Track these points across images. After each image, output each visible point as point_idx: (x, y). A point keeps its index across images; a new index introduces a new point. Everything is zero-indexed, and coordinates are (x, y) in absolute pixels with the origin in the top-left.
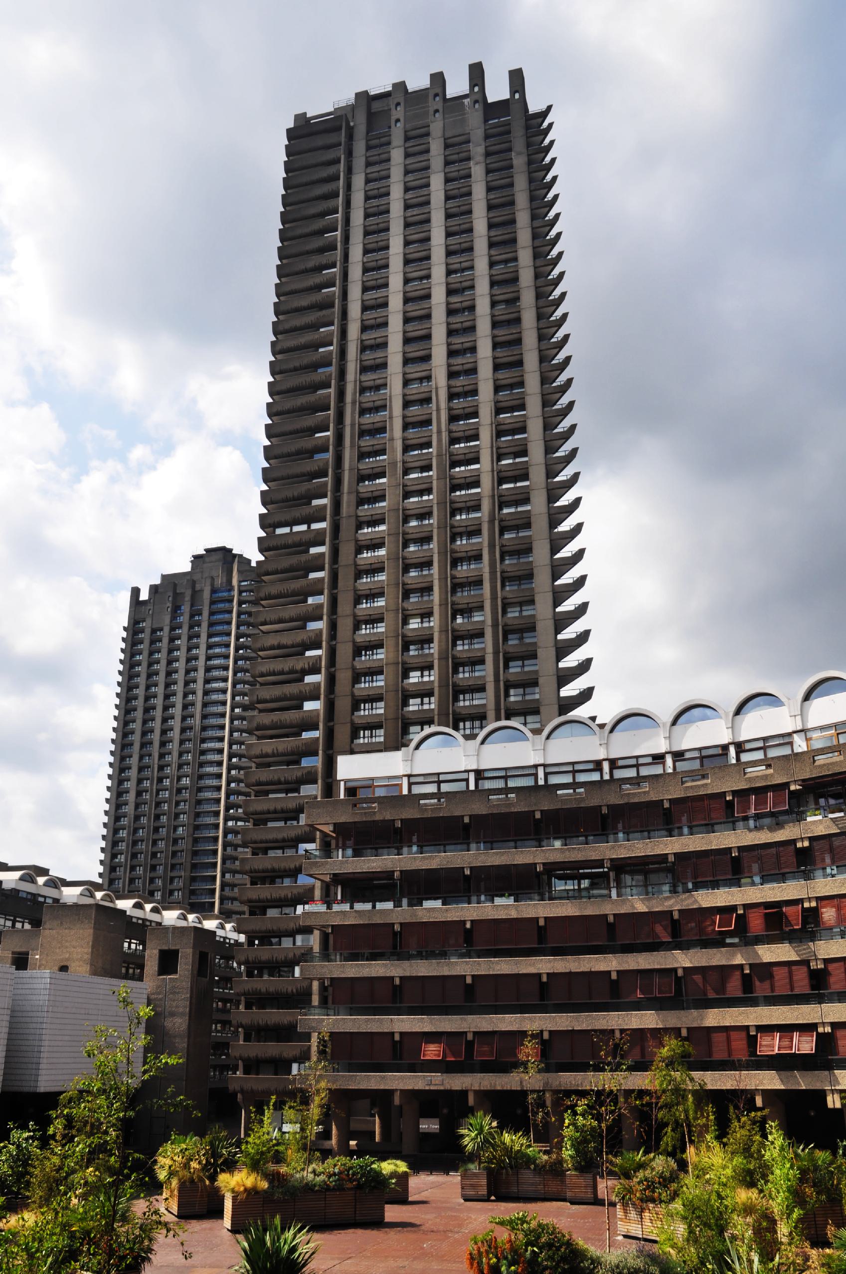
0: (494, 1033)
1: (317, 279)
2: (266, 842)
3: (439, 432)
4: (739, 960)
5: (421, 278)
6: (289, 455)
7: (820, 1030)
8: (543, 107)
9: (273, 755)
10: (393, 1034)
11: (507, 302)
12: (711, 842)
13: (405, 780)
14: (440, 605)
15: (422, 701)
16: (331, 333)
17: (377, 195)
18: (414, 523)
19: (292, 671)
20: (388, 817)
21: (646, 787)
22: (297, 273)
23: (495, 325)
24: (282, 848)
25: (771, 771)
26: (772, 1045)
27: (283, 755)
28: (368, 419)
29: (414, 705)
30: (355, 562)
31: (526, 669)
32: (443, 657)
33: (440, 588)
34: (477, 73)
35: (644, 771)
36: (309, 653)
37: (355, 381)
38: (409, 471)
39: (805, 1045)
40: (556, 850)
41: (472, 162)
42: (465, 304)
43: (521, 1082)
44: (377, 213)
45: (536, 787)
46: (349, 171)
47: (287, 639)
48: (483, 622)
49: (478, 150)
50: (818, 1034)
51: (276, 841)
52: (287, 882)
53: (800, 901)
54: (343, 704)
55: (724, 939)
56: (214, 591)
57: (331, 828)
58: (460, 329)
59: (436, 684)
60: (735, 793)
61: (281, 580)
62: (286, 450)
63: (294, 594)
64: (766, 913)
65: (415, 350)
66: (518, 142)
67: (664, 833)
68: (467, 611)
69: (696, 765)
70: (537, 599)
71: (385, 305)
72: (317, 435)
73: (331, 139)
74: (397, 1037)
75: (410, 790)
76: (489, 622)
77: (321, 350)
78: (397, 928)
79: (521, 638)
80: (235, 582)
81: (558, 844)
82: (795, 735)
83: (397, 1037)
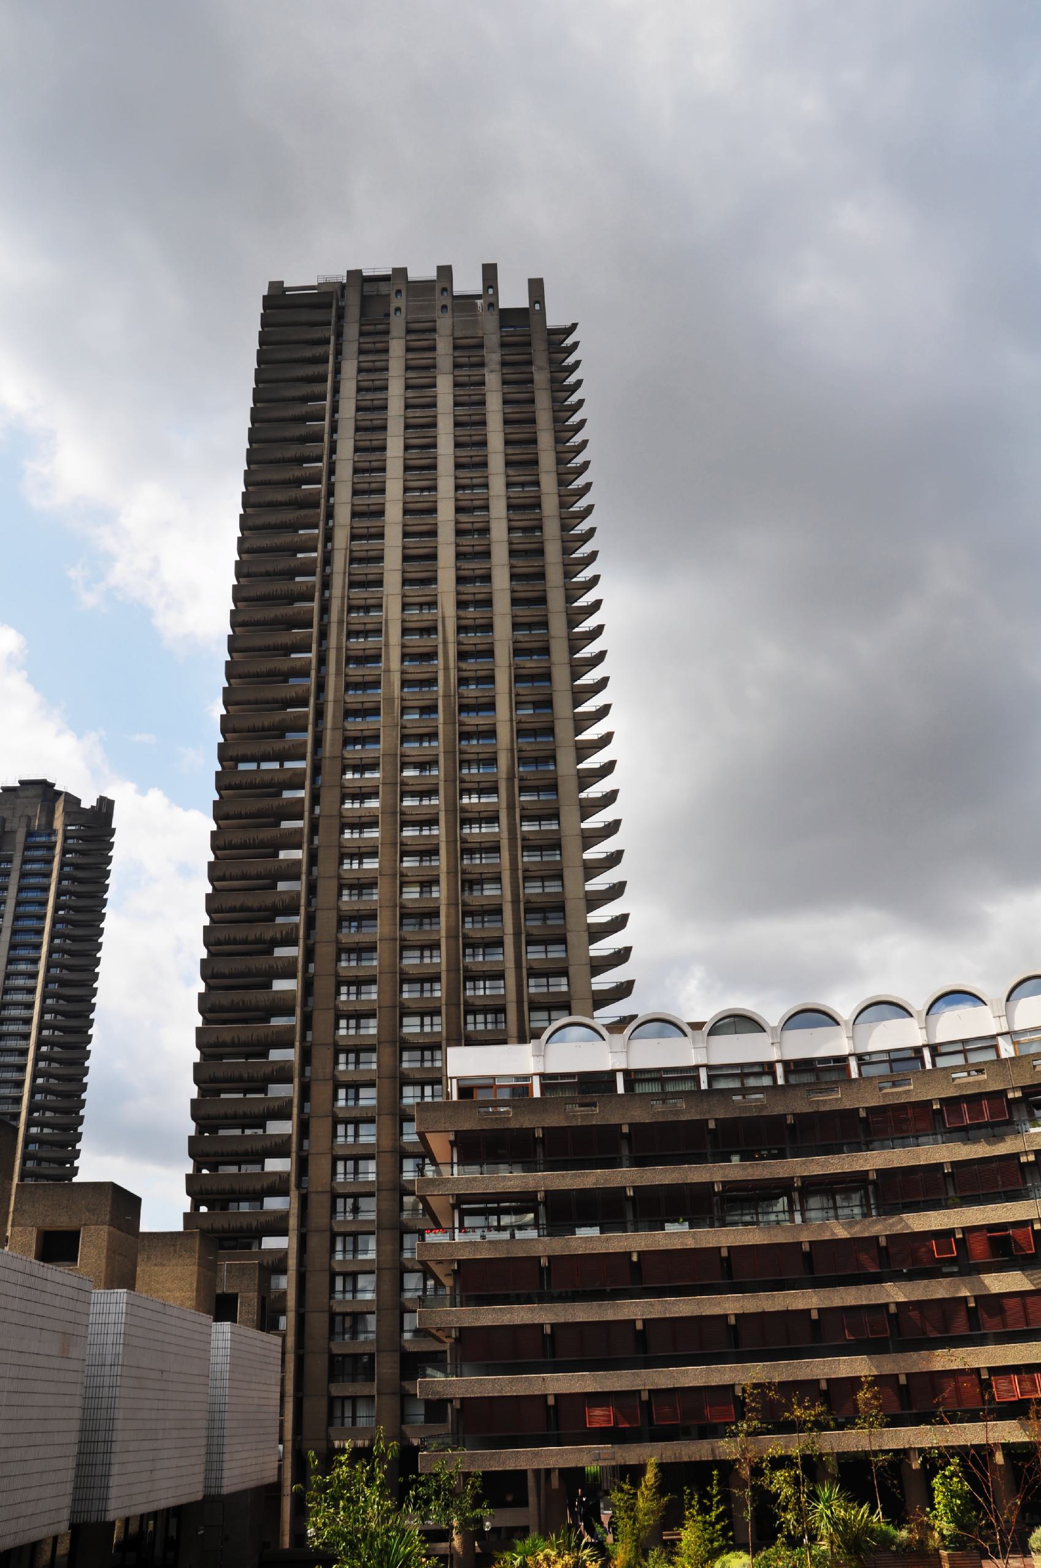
1: (297, 473)
3: (446, 668)
5: (422, 489)
6: (257, 675)
8: (568, 323)
9: (233, 1044)
10: (545, 1396)
11: (524, 530)
12: (919, 1157)
16: (315, 538)
17: (372, 389)
18: (349, 776)
19: (259, 941)
20: (527, 1125)
22: (271, 462)
23: (512, 553)
24: (239, 1164)
28: (358, 643)
30: (340, 812)
32: (452, 935)
34: (490, 273)
36: (279, 920)
37: (343, 598)
38: (406, 711)
41: (486, 369)
42: (477, 526)
43: (713, 1450)
44: (372, 409)
46: (338, 352)
47: (253, 900)
49: (493, 358)
51: (237, 1154)
52: (245, 1207)
55: (940, 1269)
56: (30, 834)
59: (444, 967)
61: (243, 827)
62: (255, 668)
63: (262, 845)
64: (990, 1238)
65: (417, 570)
66: (540, 356)
69: (884, 1069)
71: (381, 513)
72: (293, 656)
73: (318, 315)
74: (551, 1401)
75: (710, 1084)
76: (508, 896)
77: (299, 556)
78: (544, 1262)
79: (545, 919)
80: (58, 824)
82: (999, 1038)
83: (551, 1401)
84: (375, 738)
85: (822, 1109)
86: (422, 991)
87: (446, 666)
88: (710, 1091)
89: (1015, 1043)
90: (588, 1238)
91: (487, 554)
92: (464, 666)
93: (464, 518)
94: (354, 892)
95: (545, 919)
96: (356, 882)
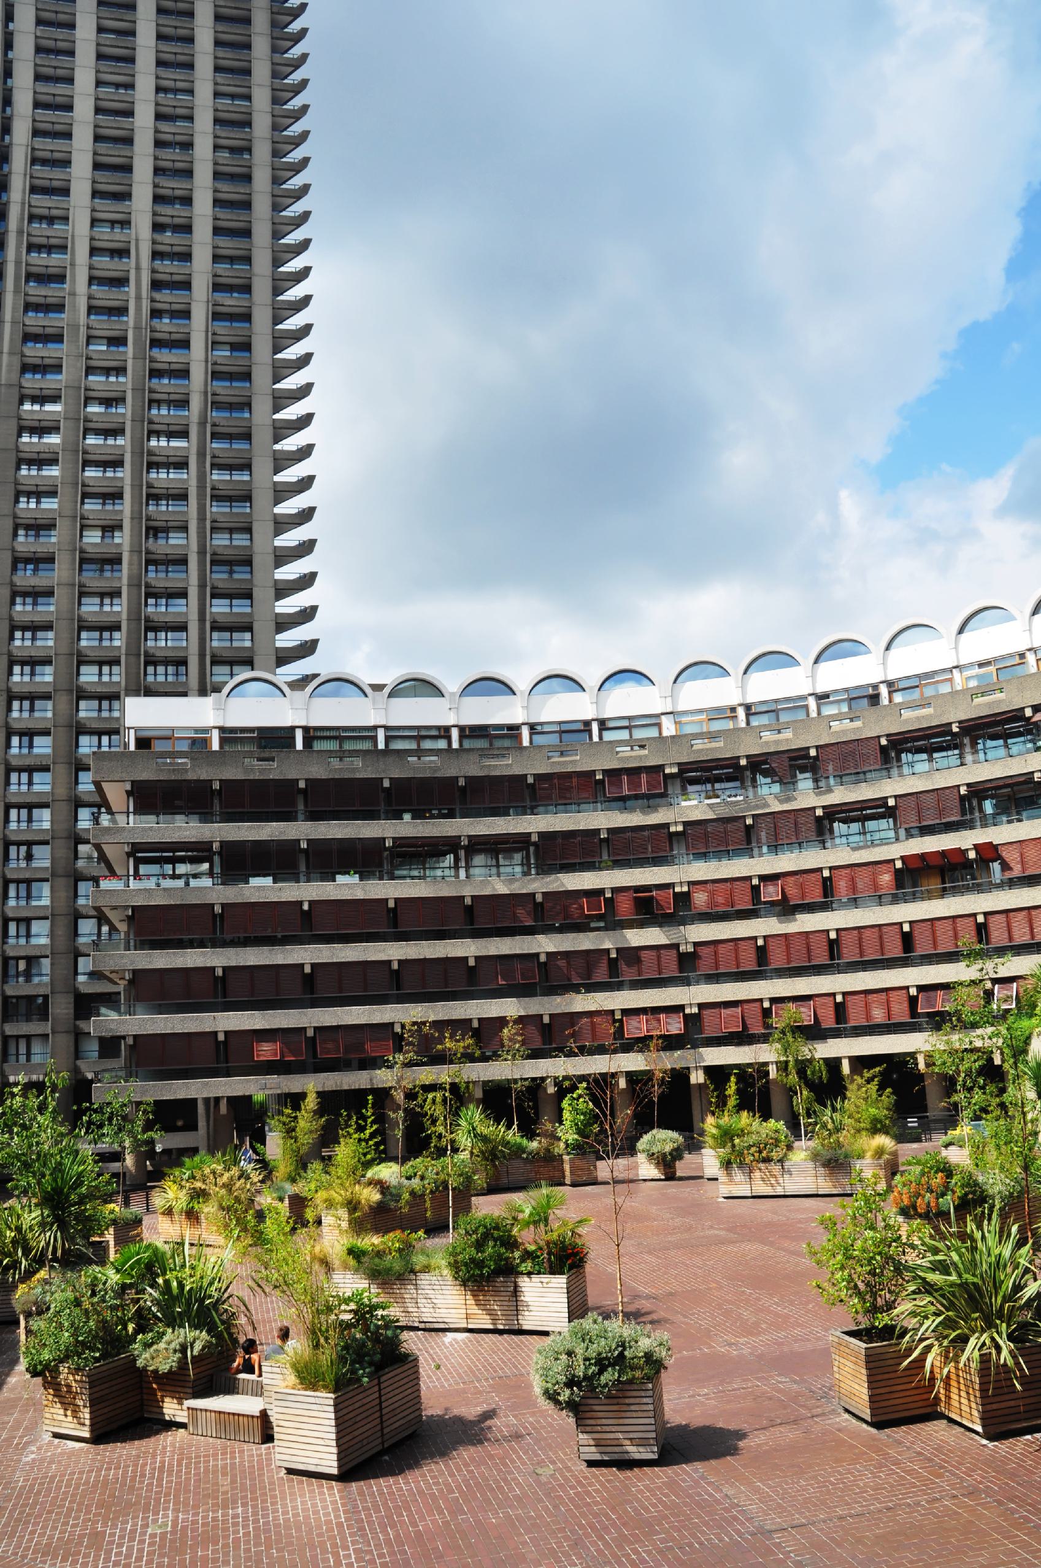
0: (338, 1027)
3: (138, 298)
4: (607, 945)
7: (688, 1011)
10: (215, 1033)
11: (232, 150)
14: (132, 518)
15: (101, 635)
18: (27, 407)
20: (204, 776)
23: (217, 175)
25: (646, 752)
26: (637, 1028)
28: (39, 259)
30: (17, 446)
31: (235, 610)
32: (135, 584)
33: (132, 497)
37: (23, 204)
38: (92, 340)
39: (675, 1026)
42: (178, 138)
50: (685, 1016)
53: (671, 885)
55: (589, 923)
58: (173, 171)
59: (124, 616)
64: (636, 898)
69: (554, 739)
76: (194, 546)
78: (218, 909)
79: (231, 572)
82: (663, 717)
84: (57, 368)
85: (493, 773)
86: (101, 639)
87: (137, 295)
88: (387, 751)
90: (261, 888)
91: (189, 173)
92: (158, 296)
93: (165, 127)
94: (30, 533)
95: (231, 572)
96: (33, 522)
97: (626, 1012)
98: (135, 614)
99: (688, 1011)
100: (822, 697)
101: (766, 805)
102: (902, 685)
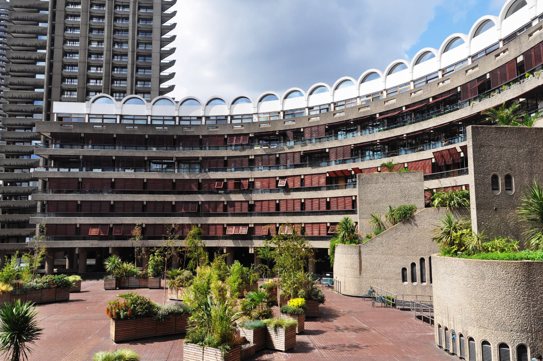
0: (122, 224)
2: (15, 139)
4: (223, 199)
7: (250, 226)
9: (19, 98)
13: (87, 116)
19: (29, 59)
20: (78, 131)
21: (193, 129)
24: (23, 142)
26: (232, 231)
27: (24, 98)
29: (92, 83)
31: (146, 73)
32: (108, 63)
35: (193, 123)
36: (39, 51)
39: (244, 231)
40: (153, 152)
45: (147, 125)
47: (27, 42)
48: (127, 49)
51: (21, 139)
52: (25, 157)
53: (248, 179)
54: (56, 78)
57: (49, 134)
59: (104, 75)
60: (228, 135)
67: (199, 148)
68: (120, 43)
70: (153, 42)
75: (89, 120)
76: (130, 50)
78: (80, 180)
79: (145, 59)
81: (154, 149)
83: (78, 226)
86: (96, 83)
88: (151, 124)
89: (259, 117)
97: (228, 225)
98: (107, 74)
99: (250, 226)
100: (310, 109)
101: (284, 150)
102: (339, 104)
